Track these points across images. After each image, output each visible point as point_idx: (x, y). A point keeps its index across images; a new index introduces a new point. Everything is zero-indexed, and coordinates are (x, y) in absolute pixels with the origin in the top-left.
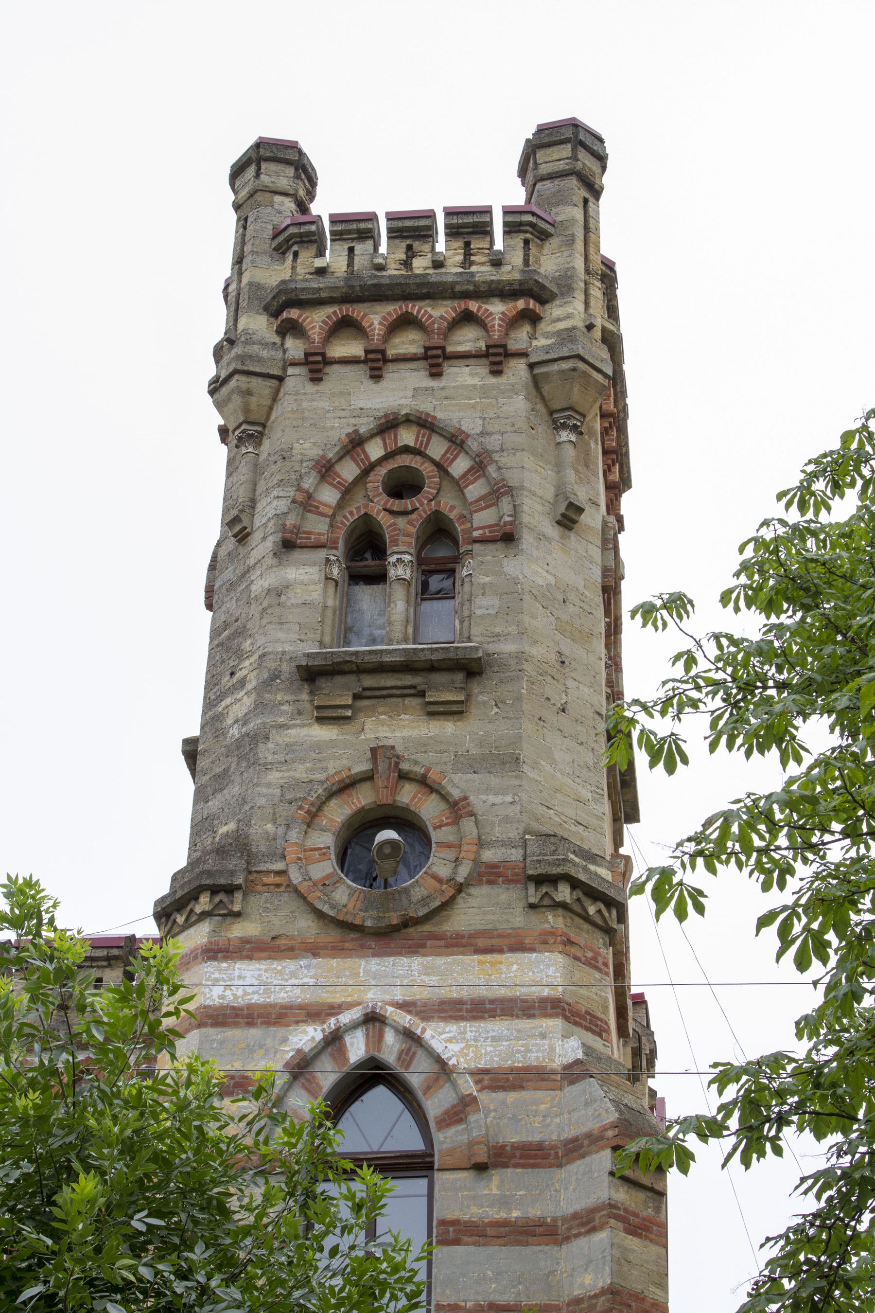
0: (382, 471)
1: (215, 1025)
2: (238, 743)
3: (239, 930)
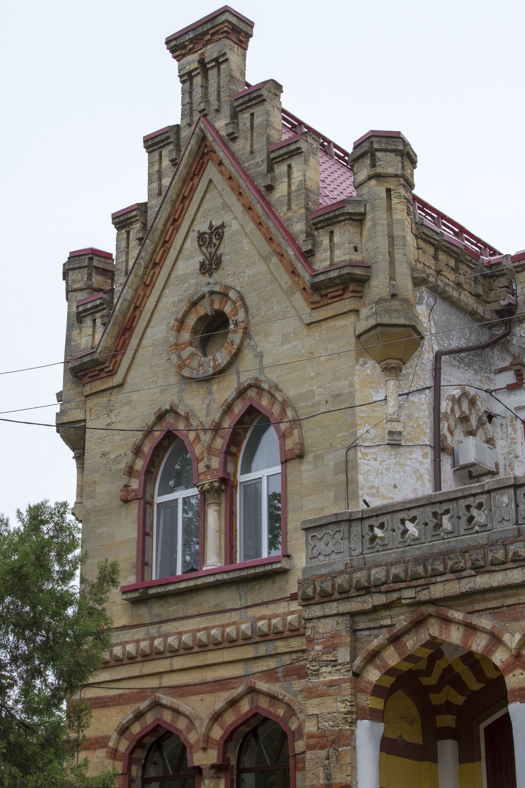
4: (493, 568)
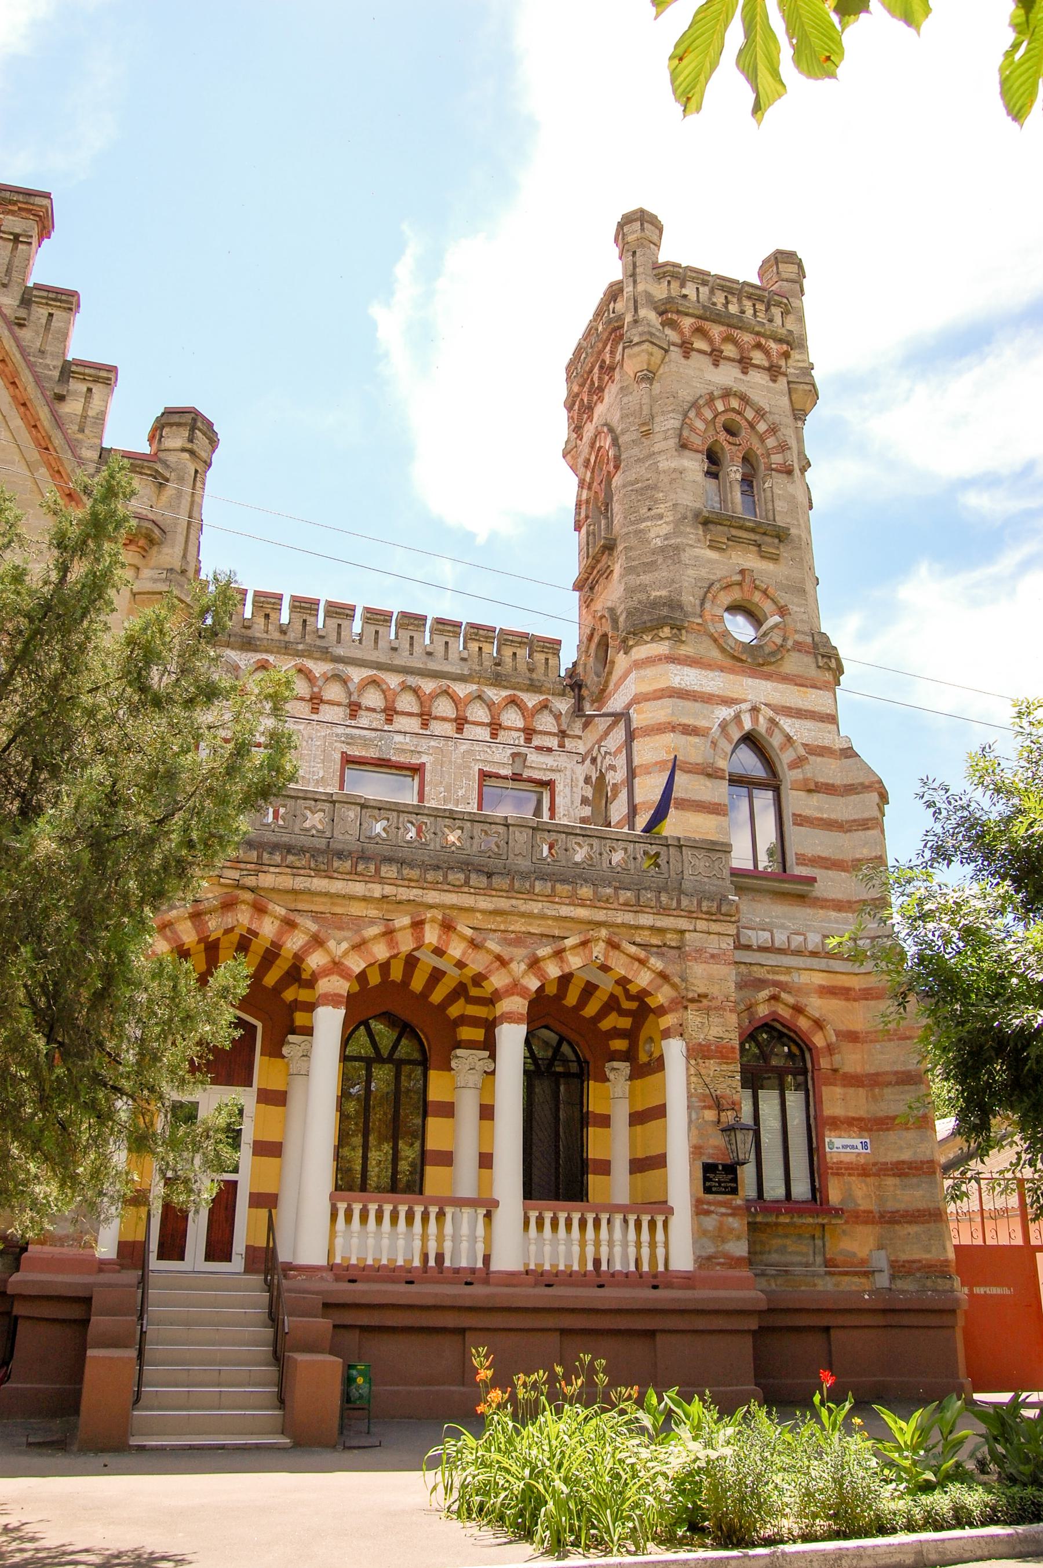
0: (722, 419)
1: (678, 697)
2: (662, 549)
3: (685, 650)
4: (335, 875)
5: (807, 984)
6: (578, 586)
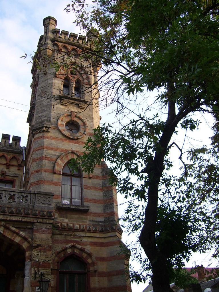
2: (47, 105)
5: (86, 241)
6: (28, 122)
